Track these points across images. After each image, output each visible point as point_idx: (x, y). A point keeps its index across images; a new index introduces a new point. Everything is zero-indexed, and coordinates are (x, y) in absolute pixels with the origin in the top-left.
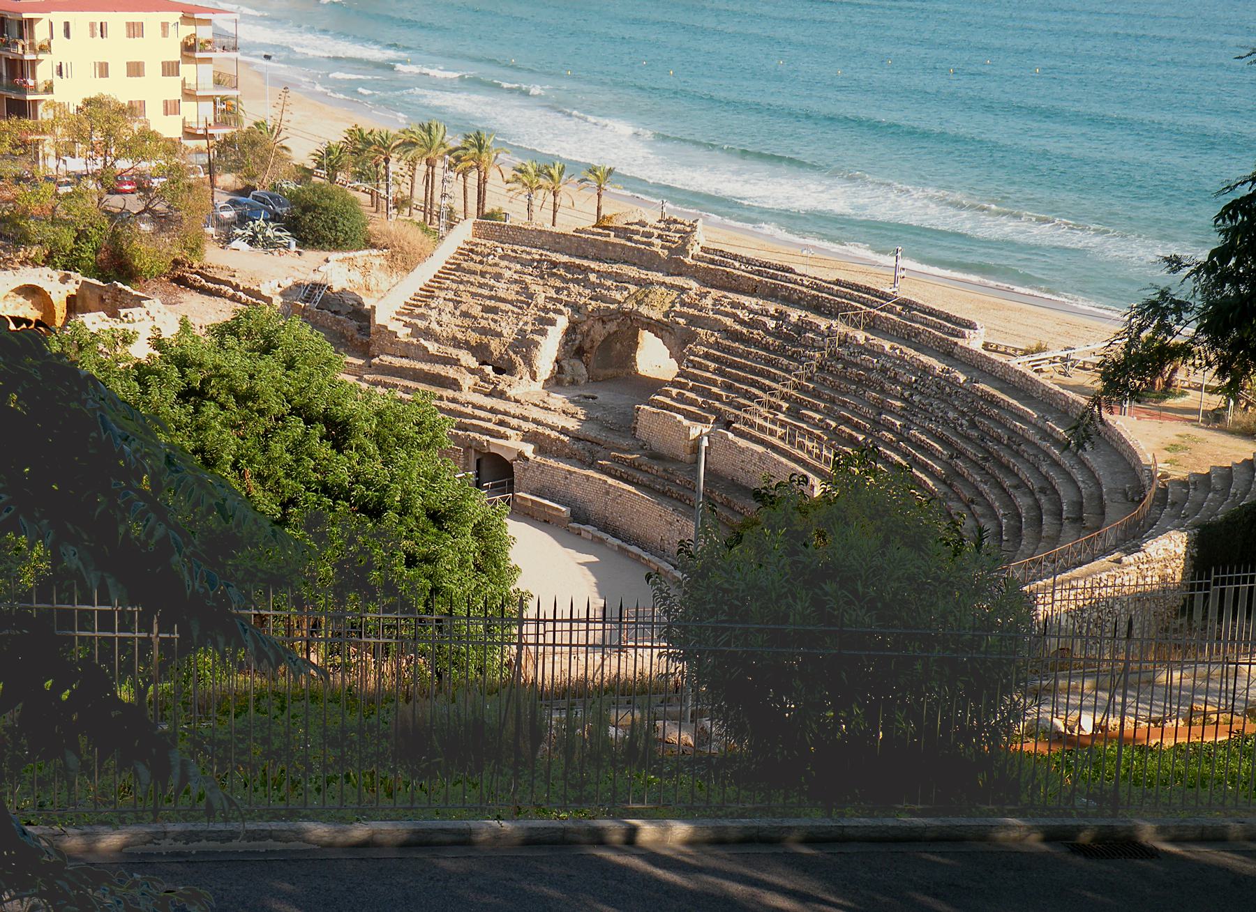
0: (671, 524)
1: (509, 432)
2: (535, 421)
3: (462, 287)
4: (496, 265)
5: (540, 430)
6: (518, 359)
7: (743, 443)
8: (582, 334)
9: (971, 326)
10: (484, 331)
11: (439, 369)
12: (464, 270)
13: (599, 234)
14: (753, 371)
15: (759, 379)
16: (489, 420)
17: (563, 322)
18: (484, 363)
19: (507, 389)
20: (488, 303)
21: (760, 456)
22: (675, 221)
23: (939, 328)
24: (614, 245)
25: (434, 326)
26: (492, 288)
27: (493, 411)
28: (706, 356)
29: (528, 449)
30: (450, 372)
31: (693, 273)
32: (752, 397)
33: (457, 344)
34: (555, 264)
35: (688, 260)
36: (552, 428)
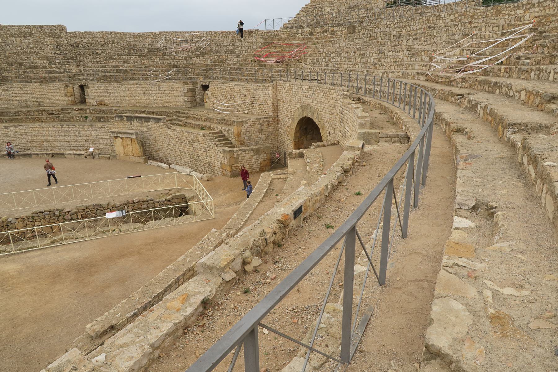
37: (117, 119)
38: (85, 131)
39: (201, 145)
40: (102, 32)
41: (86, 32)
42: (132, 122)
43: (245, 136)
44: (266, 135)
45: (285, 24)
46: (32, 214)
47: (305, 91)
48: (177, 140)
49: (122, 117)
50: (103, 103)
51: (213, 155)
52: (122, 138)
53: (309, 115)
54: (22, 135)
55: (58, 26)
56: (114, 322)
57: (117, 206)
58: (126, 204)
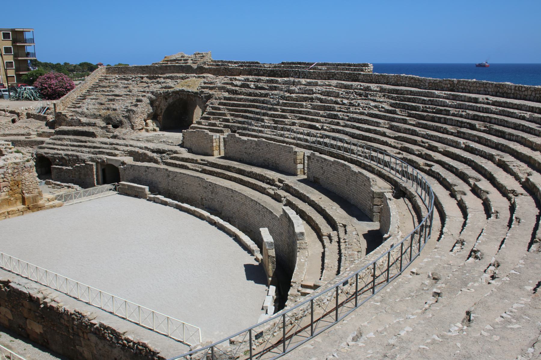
0: (206, 188)
1: (117, 152)
2: (131, 146)
3: (99, 93)
4: (116, 82)
5: (133, 149)
6: (125, 120)
7: (245, 138)
8: (156, 106)
9: (366, 65)
10: (108, 109)
11: (86, 129)
12: (100, 86)
13: (163, 64)
14: (244, 106)
15: (249, 109)
16: (108, 149)
17: (146, 100)
18: (108, 124)
19: (118, 134)
20: (111, 97)
21: (257, 143)
22: (199, 54)
23: (347, 69)
24: (169, 66)
25: (86, 111)
26: (113, 91)
27: (112, 144)
28: (220, 104)
29: (129, 160)
30: (91, 129)
31: (209, 71)
32: (247, 117)
33: (95, 116)
34: (142, 78)
35: (206, 67)
36: (141, 148)
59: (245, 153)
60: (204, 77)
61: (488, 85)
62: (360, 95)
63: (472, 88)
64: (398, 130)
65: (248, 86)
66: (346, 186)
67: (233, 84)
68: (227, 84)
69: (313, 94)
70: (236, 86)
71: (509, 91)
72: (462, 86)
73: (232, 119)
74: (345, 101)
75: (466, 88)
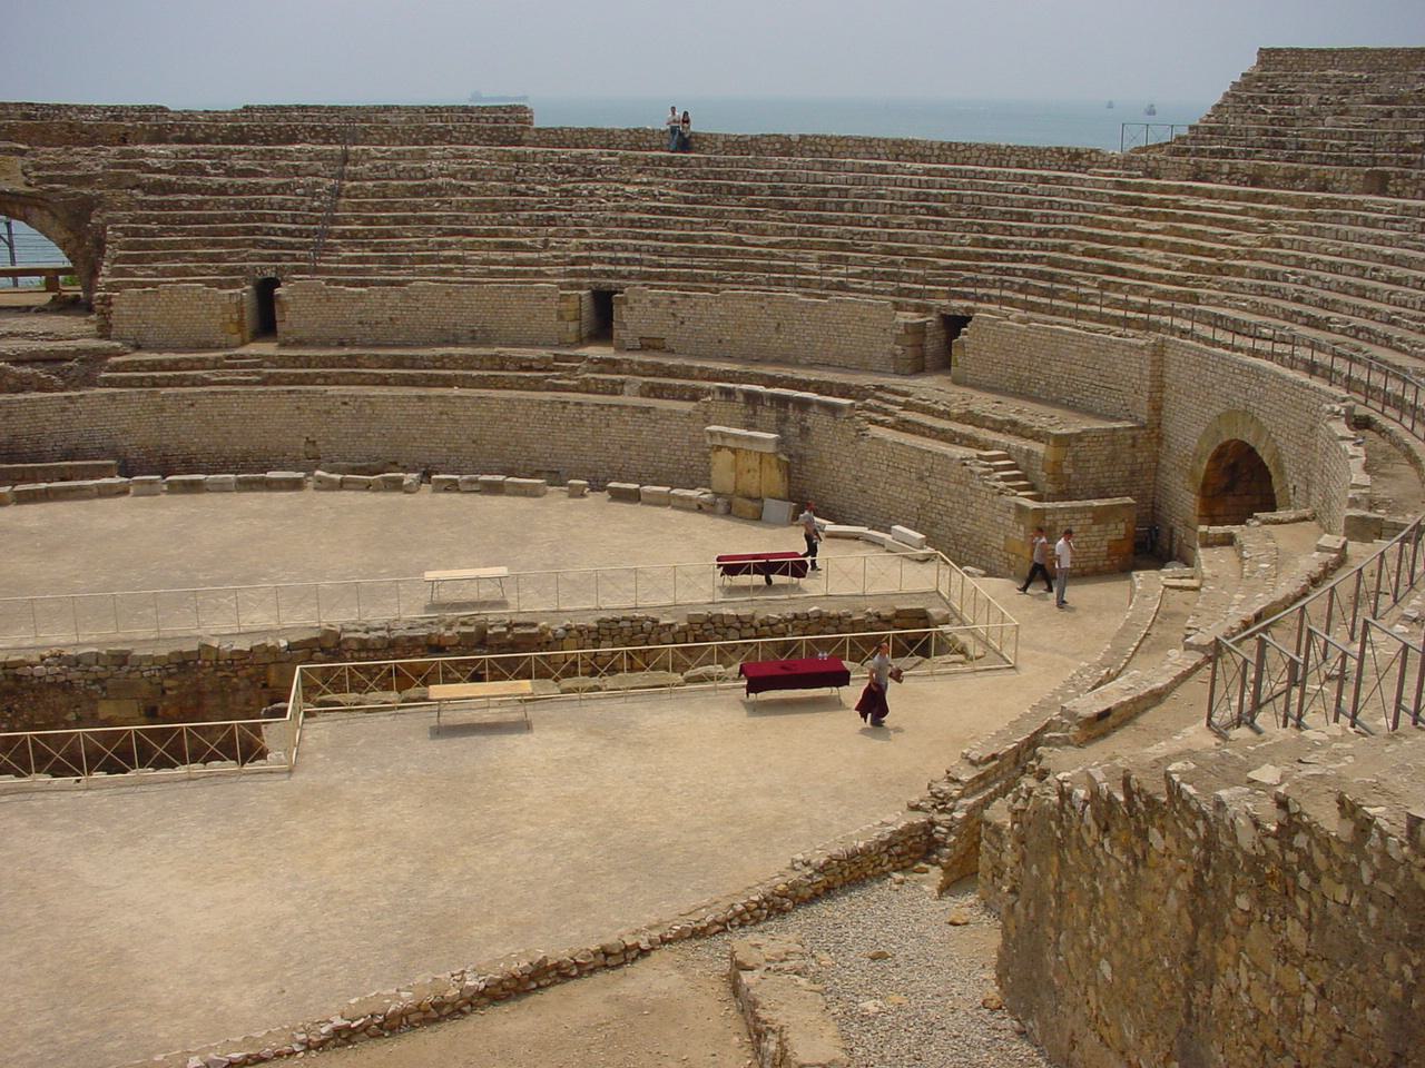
37: (717, 396)
38: (626, 423)
39: (953, 486)
40: (637, 130)
41: (592, 129)
42: (759, 408)
43: (1071, 471)
44: (1127, 474)
45: (1179, 138)
46: (598, 622)
47: (1240, 378)
48: (884, 467)
49: (729, 393)
50: (657, 344)
51: (986, 515)
52: (734, 451)
53: (1249, 438)
54: (456, 421)
55: (514, 109)
56: (994, 751)
57: (771, 622)
58: (791, 621)
59: (360, 323)
60: (22, 153)
61: (874, 143)
62: (570, 172)
63: (837, 149)
64: (763, 233)
65: (201, 171)
66: (775, 336)
67: (146, 165)
68: (125, 166)
69: (425, 178)
70: (159, 171)
71: (928, 152)
72: (811, 144)
73: (231, 254)
74: (544, 189)
75: (821, 148)
